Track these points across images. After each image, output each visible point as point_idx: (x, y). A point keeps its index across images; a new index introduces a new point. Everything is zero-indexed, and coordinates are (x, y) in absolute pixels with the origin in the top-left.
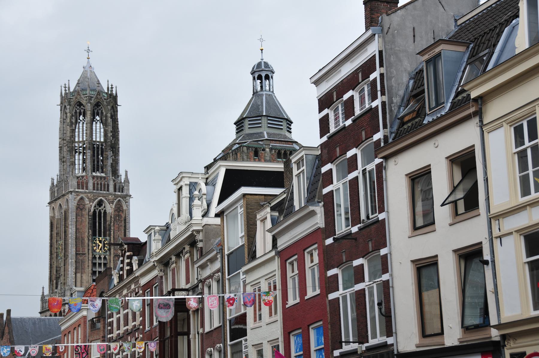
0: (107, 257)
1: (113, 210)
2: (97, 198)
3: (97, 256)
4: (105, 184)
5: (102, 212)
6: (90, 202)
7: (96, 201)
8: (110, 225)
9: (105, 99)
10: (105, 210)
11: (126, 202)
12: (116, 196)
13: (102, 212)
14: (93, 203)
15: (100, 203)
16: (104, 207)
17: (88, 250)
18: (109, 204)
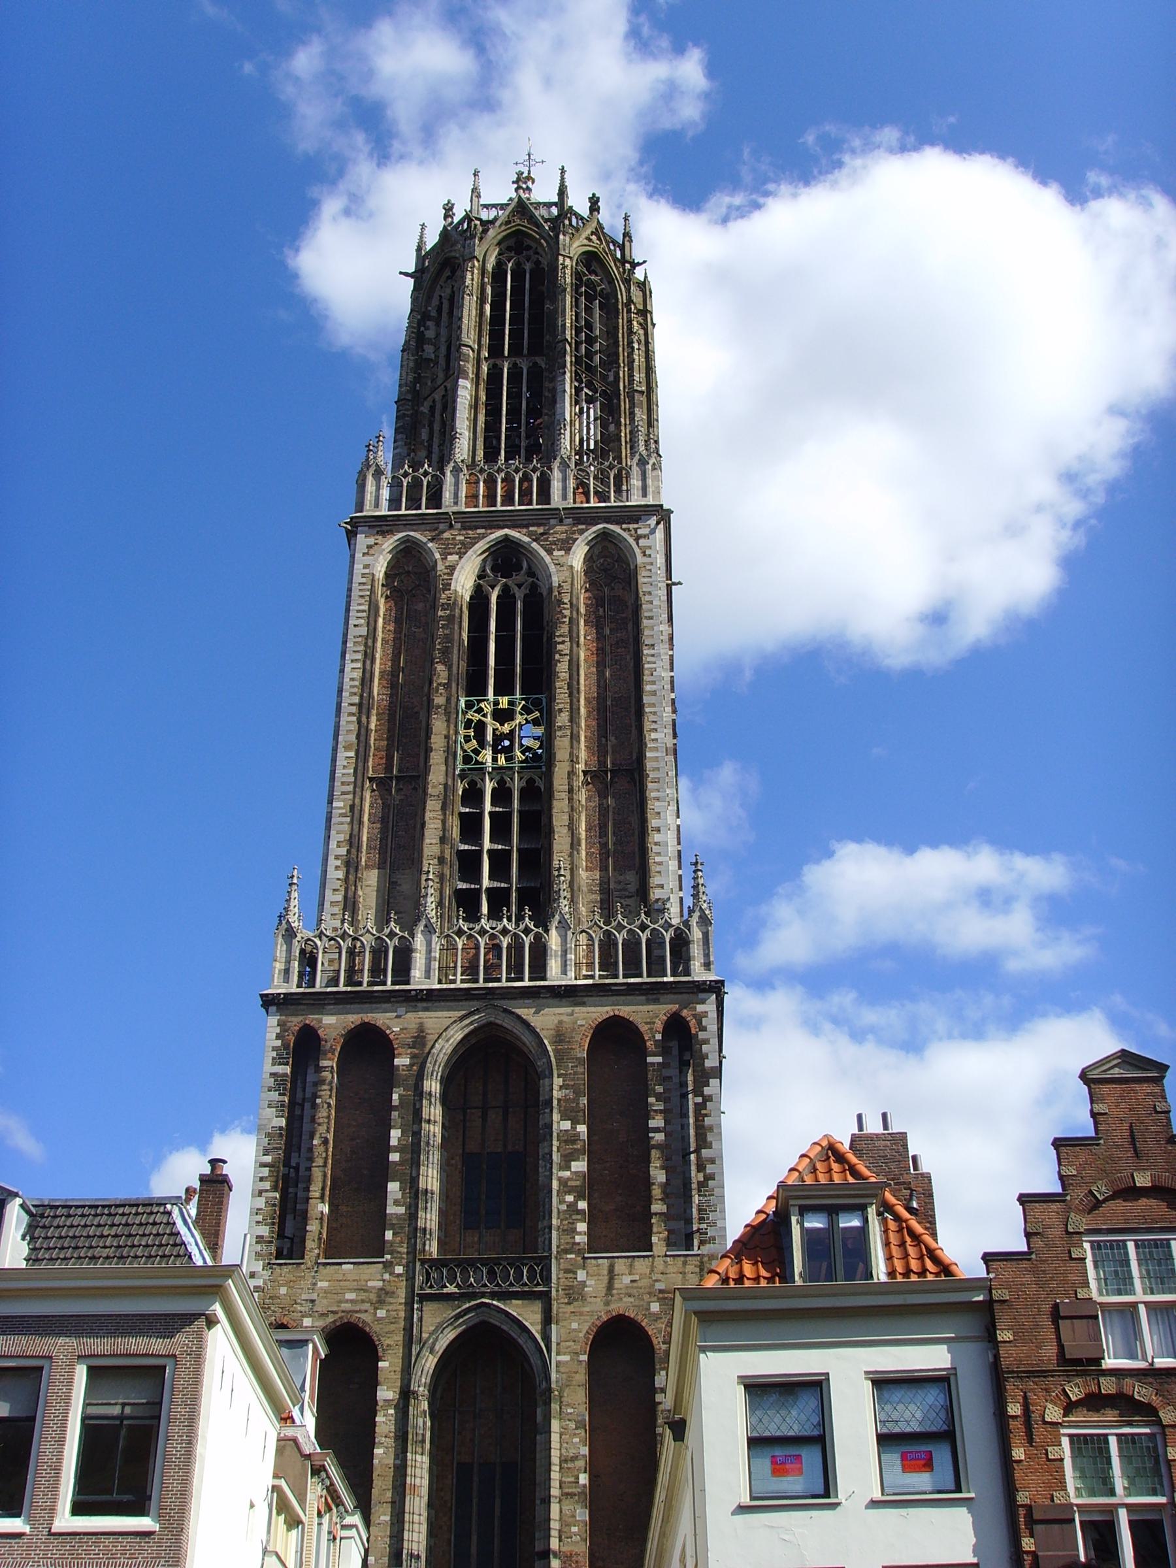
0: (541, 784)
1: (567, 574)
2: (484, 536)
3: (489, 786)
4: (526, 478)
5: (519, 594)
6: (444, 556)
7: (482, 545)
8: (551, 636)
9: (546, 221)
10: (534, 587)
11: (637, 539)
12: (582, 518)
13: (519, 594)
14: (461, 555)
15: (506, 560)
16: (531, 573)
17: (428, 750)
18: (549, 552)
